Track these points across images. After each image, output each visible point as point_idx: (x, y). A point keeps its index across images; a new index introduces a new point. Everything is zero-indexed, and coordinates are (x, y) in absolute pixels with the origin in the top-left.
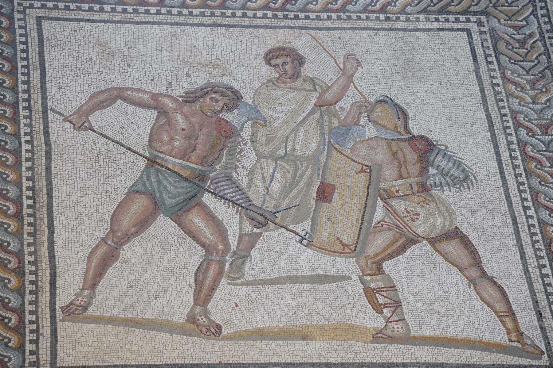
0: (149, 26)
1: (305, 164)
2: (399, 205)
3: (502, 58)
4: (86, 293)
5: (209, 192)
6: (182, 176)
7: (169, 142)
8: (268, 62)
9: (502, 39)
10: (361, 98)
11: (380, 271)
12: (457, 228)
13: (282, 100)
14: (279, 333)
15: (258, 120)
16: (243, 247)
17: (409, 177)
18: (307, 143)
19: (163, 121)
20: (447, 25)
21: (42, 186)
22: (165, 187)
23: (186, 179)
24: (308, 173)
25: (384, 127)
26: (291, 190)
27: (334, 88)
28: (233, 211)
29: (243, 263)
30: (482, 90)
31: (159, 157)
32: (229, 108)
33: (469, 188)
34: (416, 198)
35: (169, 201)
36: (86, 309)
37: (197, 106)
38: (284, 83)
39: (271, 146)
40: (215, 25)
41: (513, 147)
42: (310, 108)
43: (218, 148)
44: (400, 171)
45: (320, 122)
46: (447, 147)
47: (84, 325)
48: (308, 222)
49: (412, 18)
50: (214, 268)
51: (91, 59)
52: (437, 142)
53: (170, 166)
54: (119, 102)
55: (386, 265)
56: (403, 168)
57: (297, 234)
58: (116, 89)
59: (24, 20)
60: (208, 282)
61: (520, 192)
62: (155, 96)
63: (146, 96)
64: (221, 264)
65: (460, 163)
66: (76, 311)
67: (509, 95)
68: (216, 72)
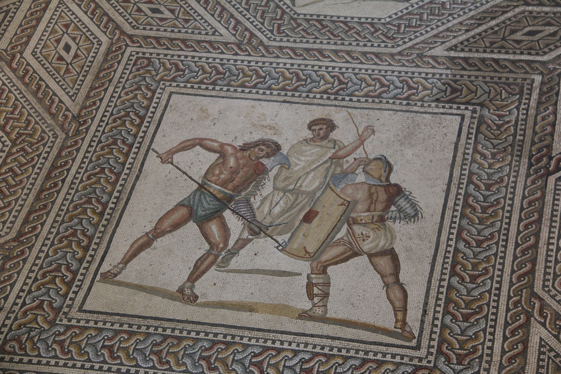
0: (239, 100)
1: (304, 196)
2: (358, 229)
3: (481, 136)
4: (121, 266)
5: (230, 209)
6: (216, 197)
7: (218, 175)
8: (310, 127)
9: (485, 122)
10: (365, 156)
11: (324, 272)
12: (393, 248)
13: (308, 153)
14: (235, 305)
15: (285, 164)
16: (236, 247)
17: (375, 211)
18: (311, 183)
19: (221, 161)
20: (450, 111)
21: (125, 197)
22: (202, 204)
23: (218, 200)
24: (304, 202)
25: (372, 176)
26: (287, 212)
27: (348, 148)
28: (240, 223)
29: (232, 257)
30: (455, 157)
31: (207, 184)
32: (268, 156)
33: (414, 222)
34: (372, 226)
35: (200, 212)
36: (116, 275)
37: (247, 154)
38: (314, 142)
39: (286, 183)
40: (284, 102)
41: (460, 197)
42: (325, 159)
43: (249, 181)
44: (369, 207)
45: (328, 170)
46: (411, 193)
47: (109, 286)
48: (289, 235)
49: (426, 104)
50: (211, 258)
51: (192, 119)
52: (405, 189)
53: (211, 190)
54: (198, 147)
55: (330, 270)
56: (373, 205)
57: (277, 242)
58: (199, 139)
59: (161, 94)
60: (202, 268)
61: (451, 228)
62: (222, 145)
63: (216, 145)
64: (216, 257)
65: (416, 204)
66: (109, 278)
67: (473, 161)
68: (270, 132)
